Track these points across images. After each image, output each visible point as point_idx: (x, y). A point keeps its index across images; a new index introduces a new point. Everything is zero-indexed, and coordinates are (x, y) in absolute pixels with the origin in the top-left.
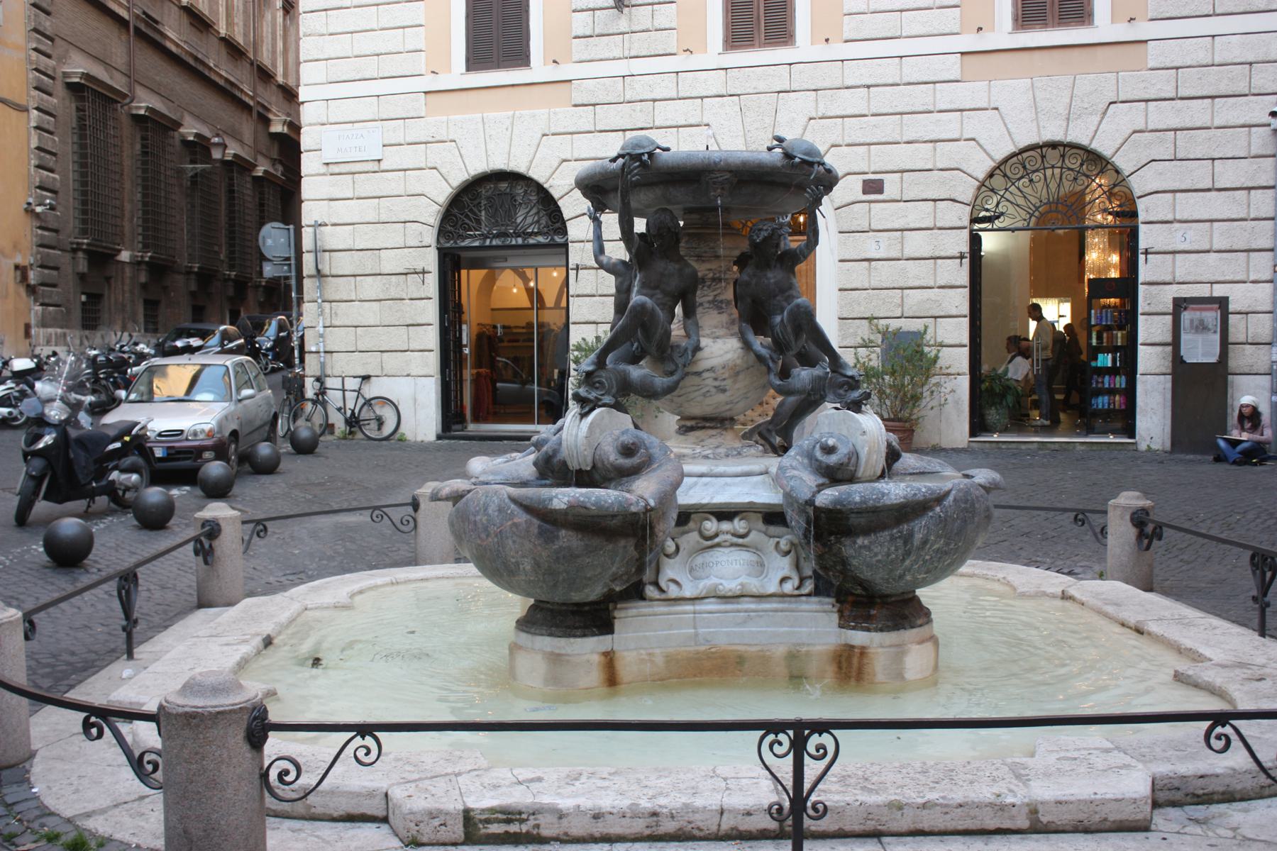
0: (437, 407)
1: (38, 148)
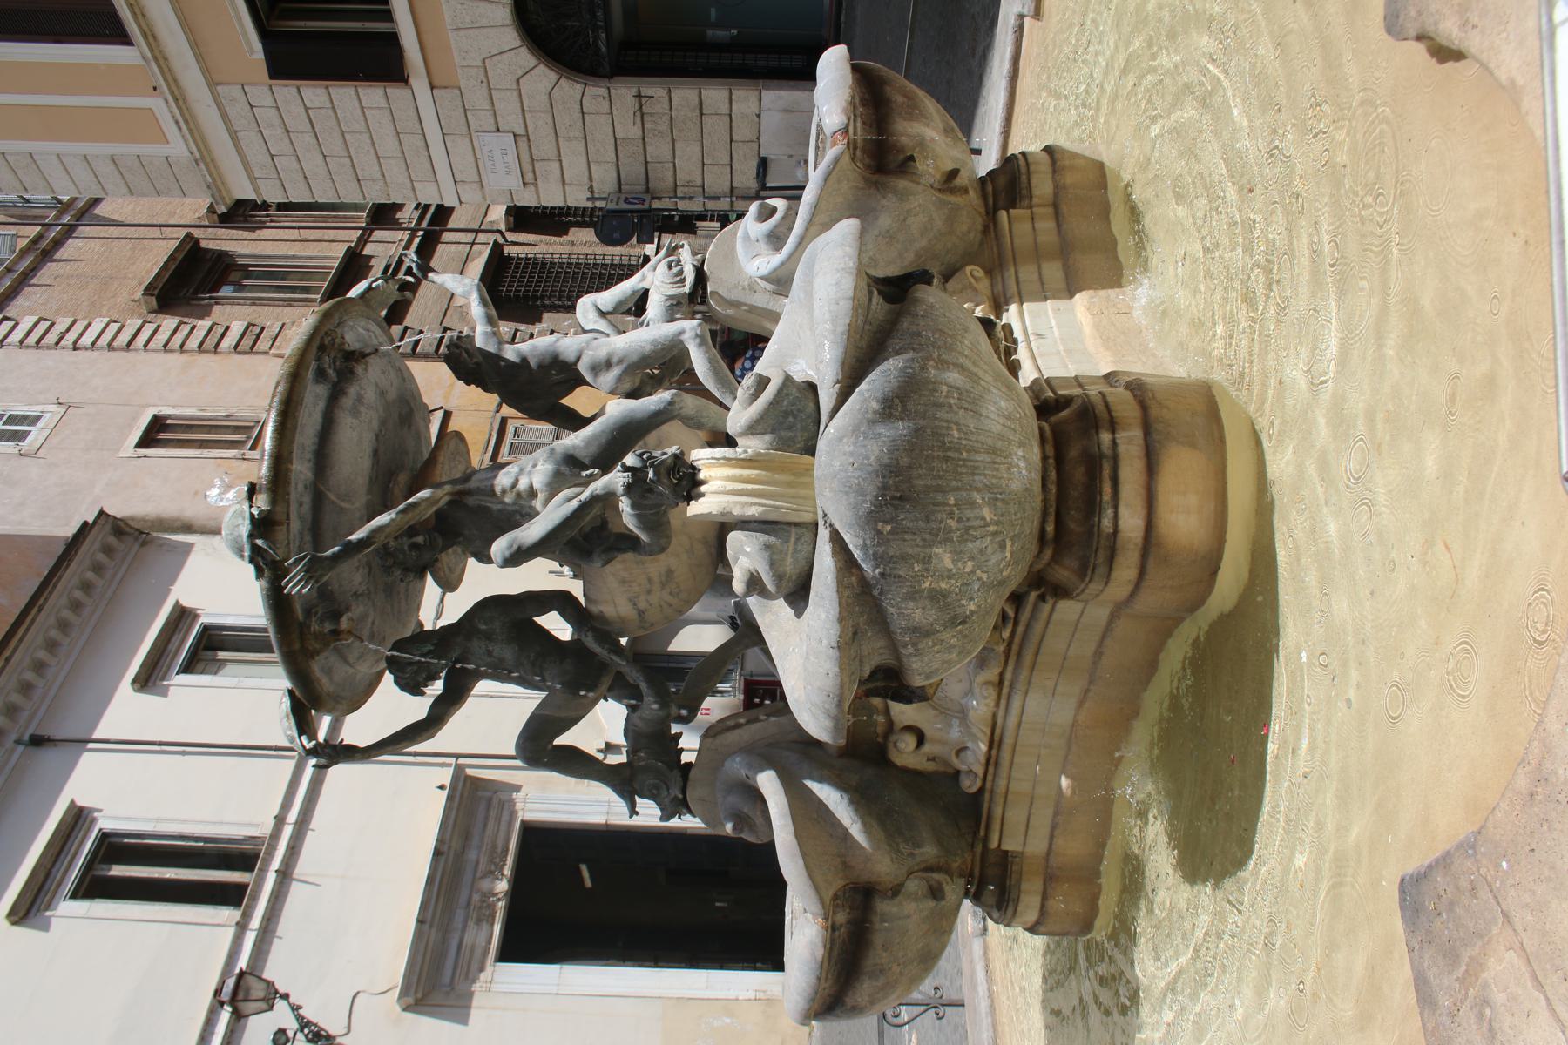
0: (798, 89)
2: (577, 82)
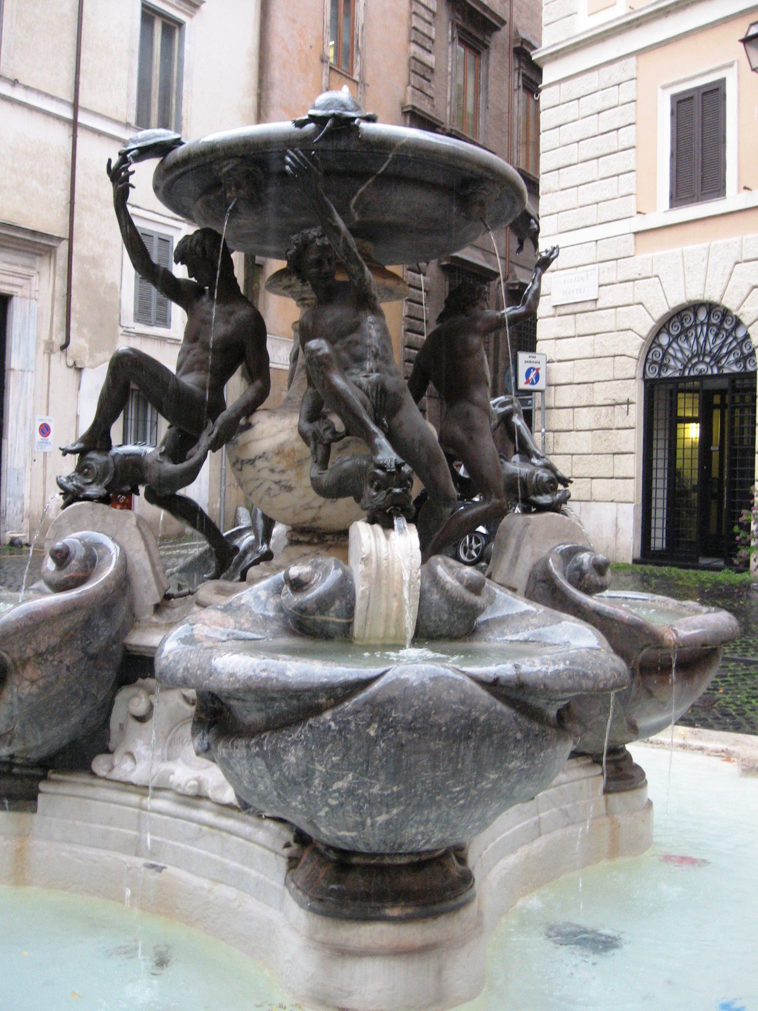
1: (409, 316)
2: (640, 353)
